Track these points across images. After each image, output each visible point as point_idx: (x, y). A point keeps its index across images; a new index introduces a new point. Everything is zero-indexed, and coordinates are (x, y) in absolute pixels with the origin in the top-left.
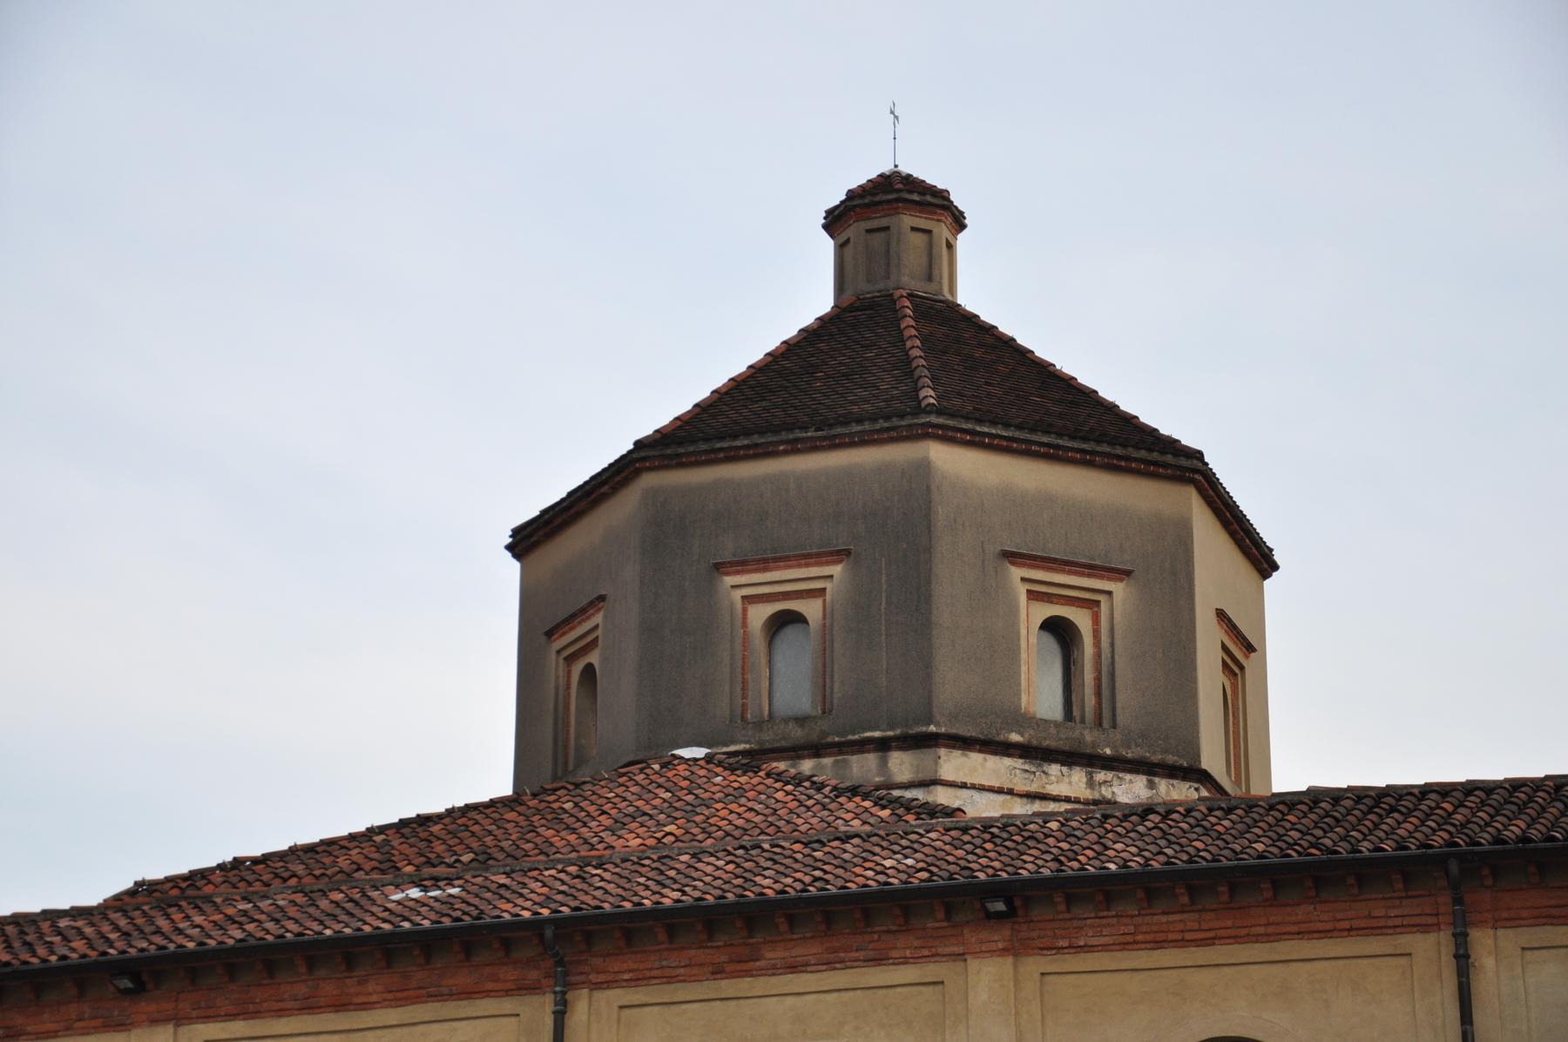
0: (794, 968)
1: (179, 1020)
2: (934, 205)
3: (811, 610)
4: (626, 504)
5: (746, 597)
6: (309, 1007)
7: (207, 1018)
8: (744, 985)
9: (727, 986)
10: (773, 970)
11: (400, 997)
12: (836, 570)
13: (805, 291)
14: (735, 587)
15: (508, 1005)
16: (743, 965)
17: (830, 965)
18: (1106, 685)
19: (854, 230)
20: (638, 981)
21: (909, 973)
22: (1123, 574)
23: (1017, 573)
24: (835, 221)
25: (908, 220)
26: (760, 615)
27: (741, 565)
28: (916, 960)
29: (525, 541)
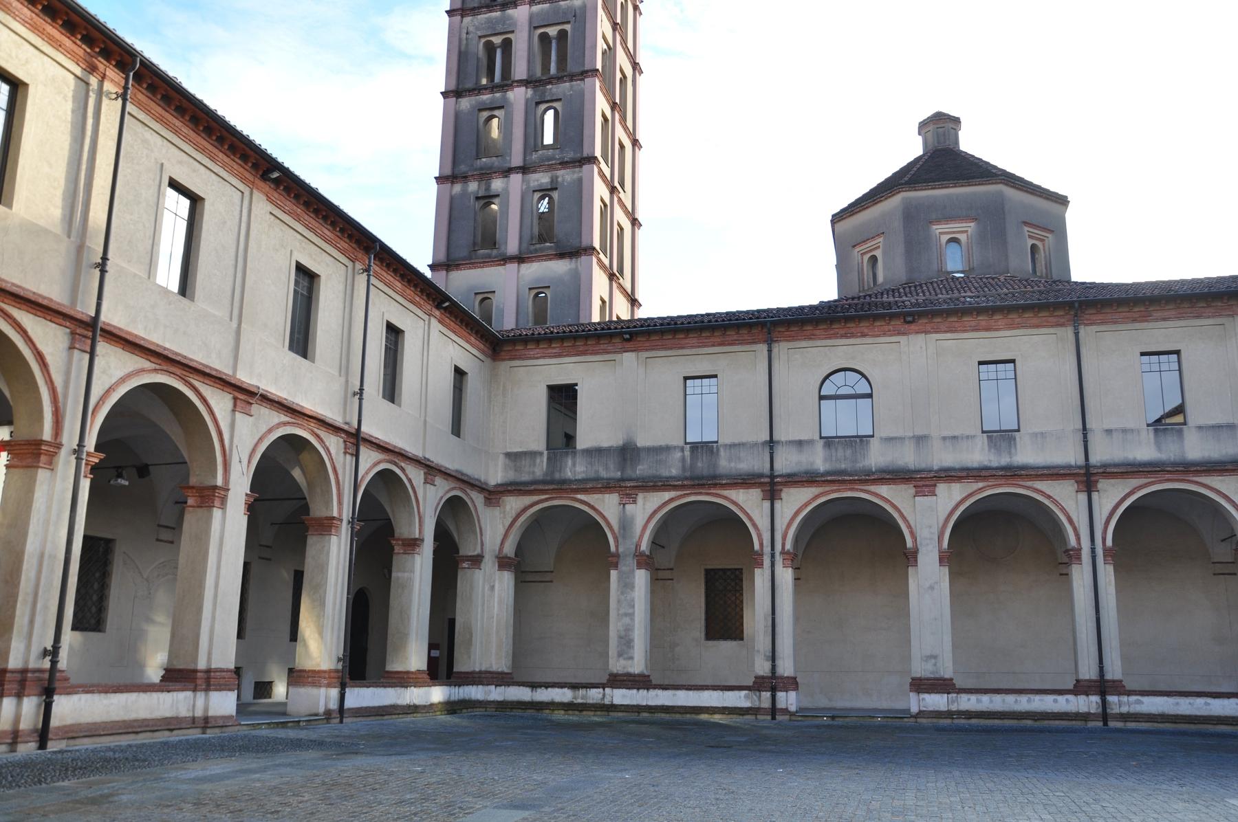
0: (1164, 319)
1: (926, 332)
2: (956, 121)
3: (963, 237)
4: (895, 202)
5: (942, 231)
6: (976, 329)
7: (936, 332)
8: (1144, 325)
9: (1137, 325)
10: (1157, 320)
11: (1011, 327)
12: (972, 224)
13: (912, 148)
14: (937, 229)
15: (1052, 330)
16: (1145, 318)
17: (1179, 318)
18: (1048, 265)
19: (931, 127)
20: (1103, 323)
21: (1211, 321)
22: (1051, 231)
23: (1026, 229)
24: (923, 125)
25: (951, 125)
26: (945, 238)
27: (938, 221)
28: (1213, 317)
29: (837, 219)
